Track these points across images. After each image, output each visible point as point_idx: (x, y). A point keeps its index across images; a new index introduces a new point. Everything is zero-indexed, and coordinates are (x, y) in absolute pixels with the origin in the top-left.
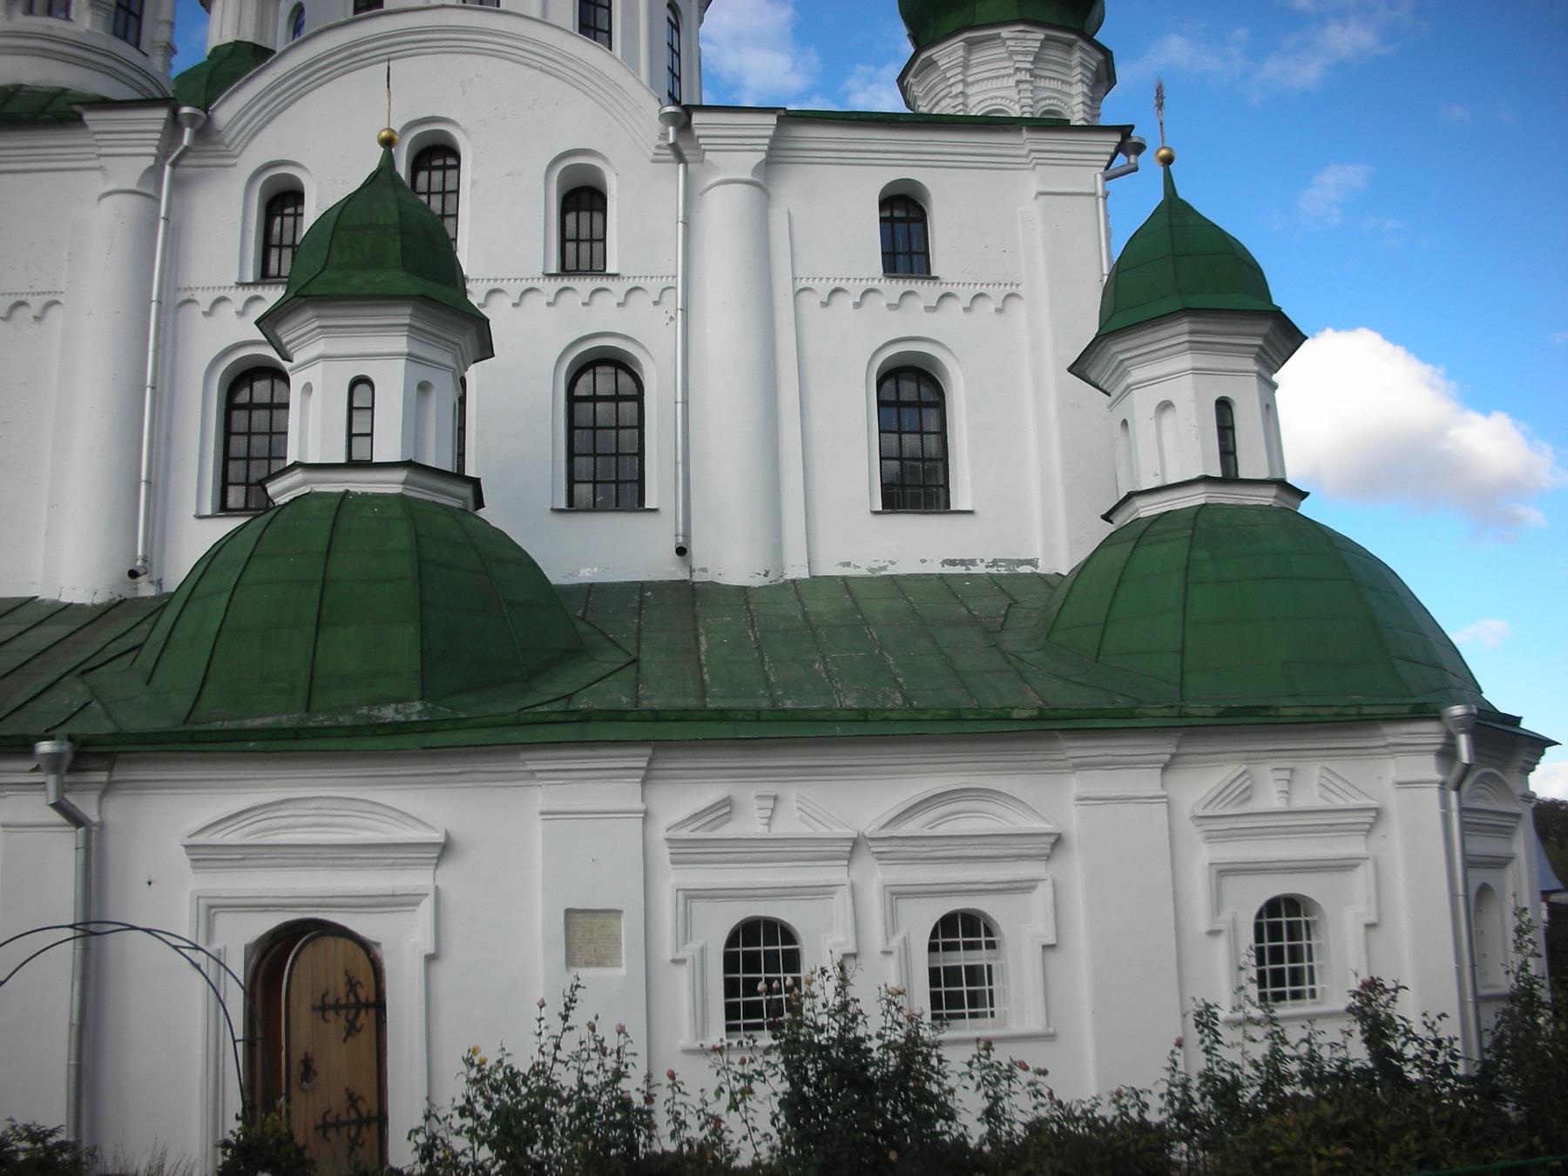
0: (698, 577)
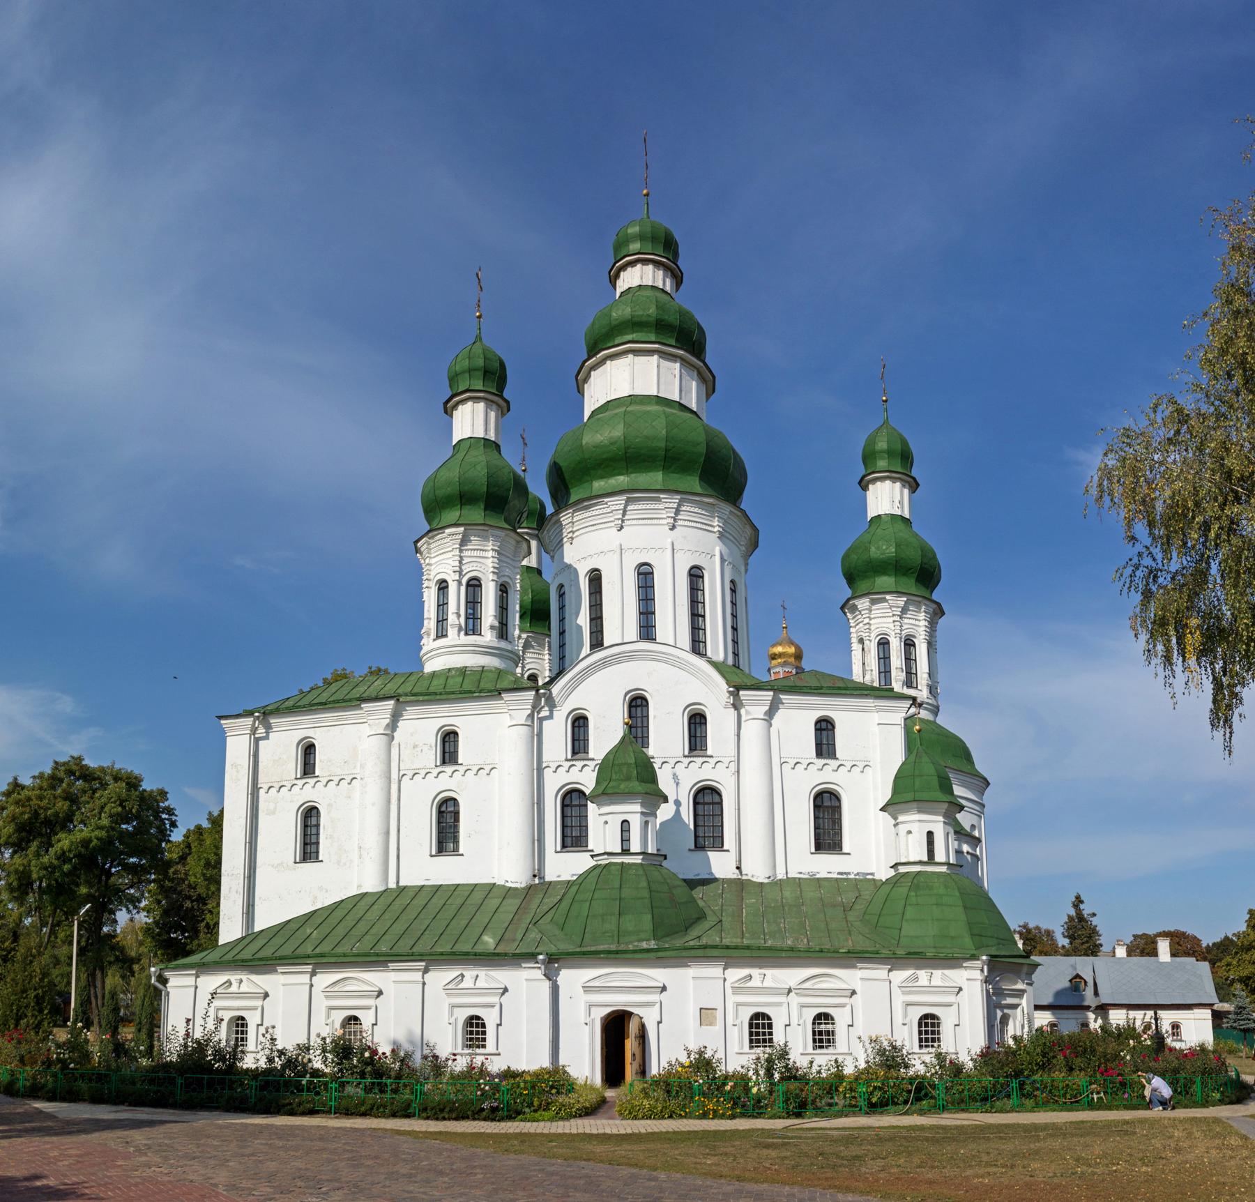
0: (744, 878)
